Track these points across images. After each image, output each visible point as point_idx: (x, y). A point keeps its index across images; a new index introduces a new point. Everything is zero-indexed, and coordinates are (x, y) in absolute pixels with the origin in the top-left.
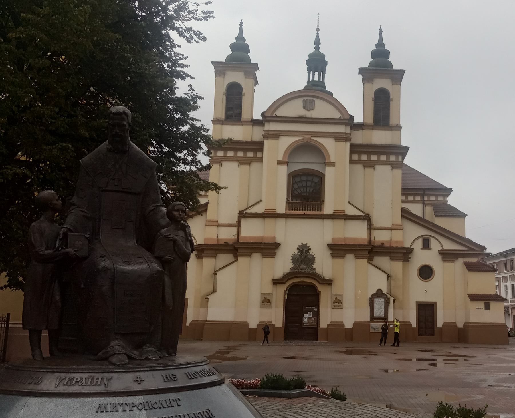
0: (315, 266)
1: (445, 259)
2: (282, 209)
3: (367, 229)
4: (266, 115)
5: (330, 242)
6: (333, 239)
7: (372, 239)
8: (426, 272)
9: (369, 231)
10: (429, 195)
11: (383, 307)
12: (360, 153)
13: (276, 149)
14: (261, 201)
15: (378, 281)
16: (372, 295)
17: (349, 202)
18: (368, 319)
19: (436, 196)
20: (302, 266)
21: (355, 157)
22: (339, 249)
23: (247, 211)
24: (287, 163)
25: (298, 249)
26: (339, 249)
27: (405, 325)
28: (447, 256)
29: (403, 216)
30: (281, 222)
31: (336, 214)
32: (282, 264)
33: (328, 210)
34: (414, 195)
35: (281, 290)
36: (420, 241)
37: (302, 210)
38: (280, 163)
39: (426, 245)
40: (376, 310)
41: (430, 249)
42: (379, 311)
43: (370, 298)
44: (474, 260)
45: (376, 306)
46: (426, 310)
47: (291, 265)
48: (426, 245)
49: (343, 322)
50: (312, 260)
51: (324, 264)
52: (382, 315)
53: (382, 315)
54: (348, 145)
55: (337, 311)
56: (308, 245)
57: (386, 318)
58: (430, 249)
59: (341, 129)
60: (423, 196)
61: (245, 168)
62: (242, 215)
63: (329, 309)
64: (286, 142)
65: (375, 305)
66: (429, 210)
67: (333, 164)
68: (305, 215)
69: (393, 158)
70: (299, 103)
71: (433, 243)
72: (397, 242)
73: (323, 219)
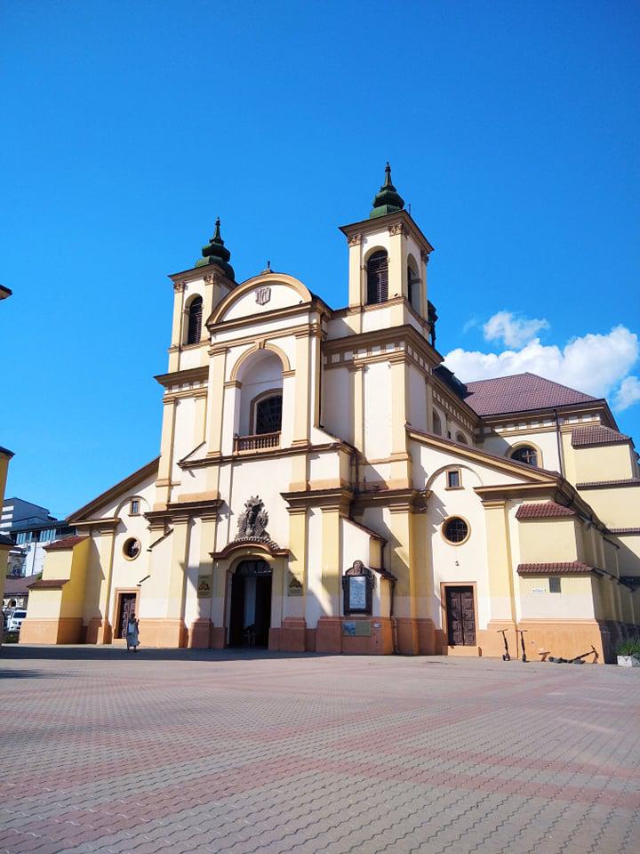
0: (267, 529)
1: (485, 503)
2: (228, 451)
3: (351, 465)
4: (210, 323)
5: (287, 491)
6: (290, 485)
7: (361, 480)
8: (456, 530)
9: (354, 468)
10: (566, 417)
11: (364, 592)
12: (342, 351)
13: (222, 369)
14: (204, 442)
15: (359, 547)
16: (347, 572)
17: (321, 427)
18: (342, 615)
19: (580, 416)
20: (249, 531)
21: (336, 358)
22: (301, 501)
23: (189, 460)
24: (238, 385)
25: (245, 505)
26: (301, 501)
27: (423, 624)
28: (489, 496)
29: (409, 438)
30: (227, 469)
31: (294, 446)
32: (227, 531)
33: (286, 441)
34: (541, 421)
35: (223, 568)
36: (443, 477)
37: (256, 448)
38: (226, 385)
39: (454, 481)
40: (351, 597)
41: (462, 488)
42: (358, 601)
43: (343, 577)
44: (545, 502)
45: (352, 591)
46: (459, 598)
47: (235, 531)
48: (454, 481)
49: (304, 619)
50: (265, 522)
51: (282, 528)
52: (362, 604)
53: (362, 604)
54: (314, 340)
55: (295, 599)
56: (259, 499)
57: (368, 610)
58: (462, 488)
59: (304, 319)
60: (553, 419)
61: (203, 401)
62: (186, 465)
63: (285, 597)
64: (236, 354)
65: (351, 589)
66: (567, 439)
67: (292, 373)
68: (257, 454)
69: (391, 350)
70: (252, 296)
71: (464, 473)
72: (398, 481)
73: (279, 457)
